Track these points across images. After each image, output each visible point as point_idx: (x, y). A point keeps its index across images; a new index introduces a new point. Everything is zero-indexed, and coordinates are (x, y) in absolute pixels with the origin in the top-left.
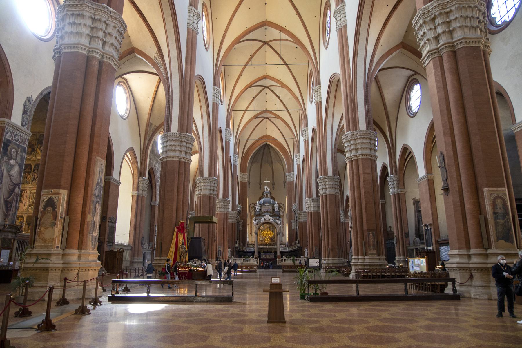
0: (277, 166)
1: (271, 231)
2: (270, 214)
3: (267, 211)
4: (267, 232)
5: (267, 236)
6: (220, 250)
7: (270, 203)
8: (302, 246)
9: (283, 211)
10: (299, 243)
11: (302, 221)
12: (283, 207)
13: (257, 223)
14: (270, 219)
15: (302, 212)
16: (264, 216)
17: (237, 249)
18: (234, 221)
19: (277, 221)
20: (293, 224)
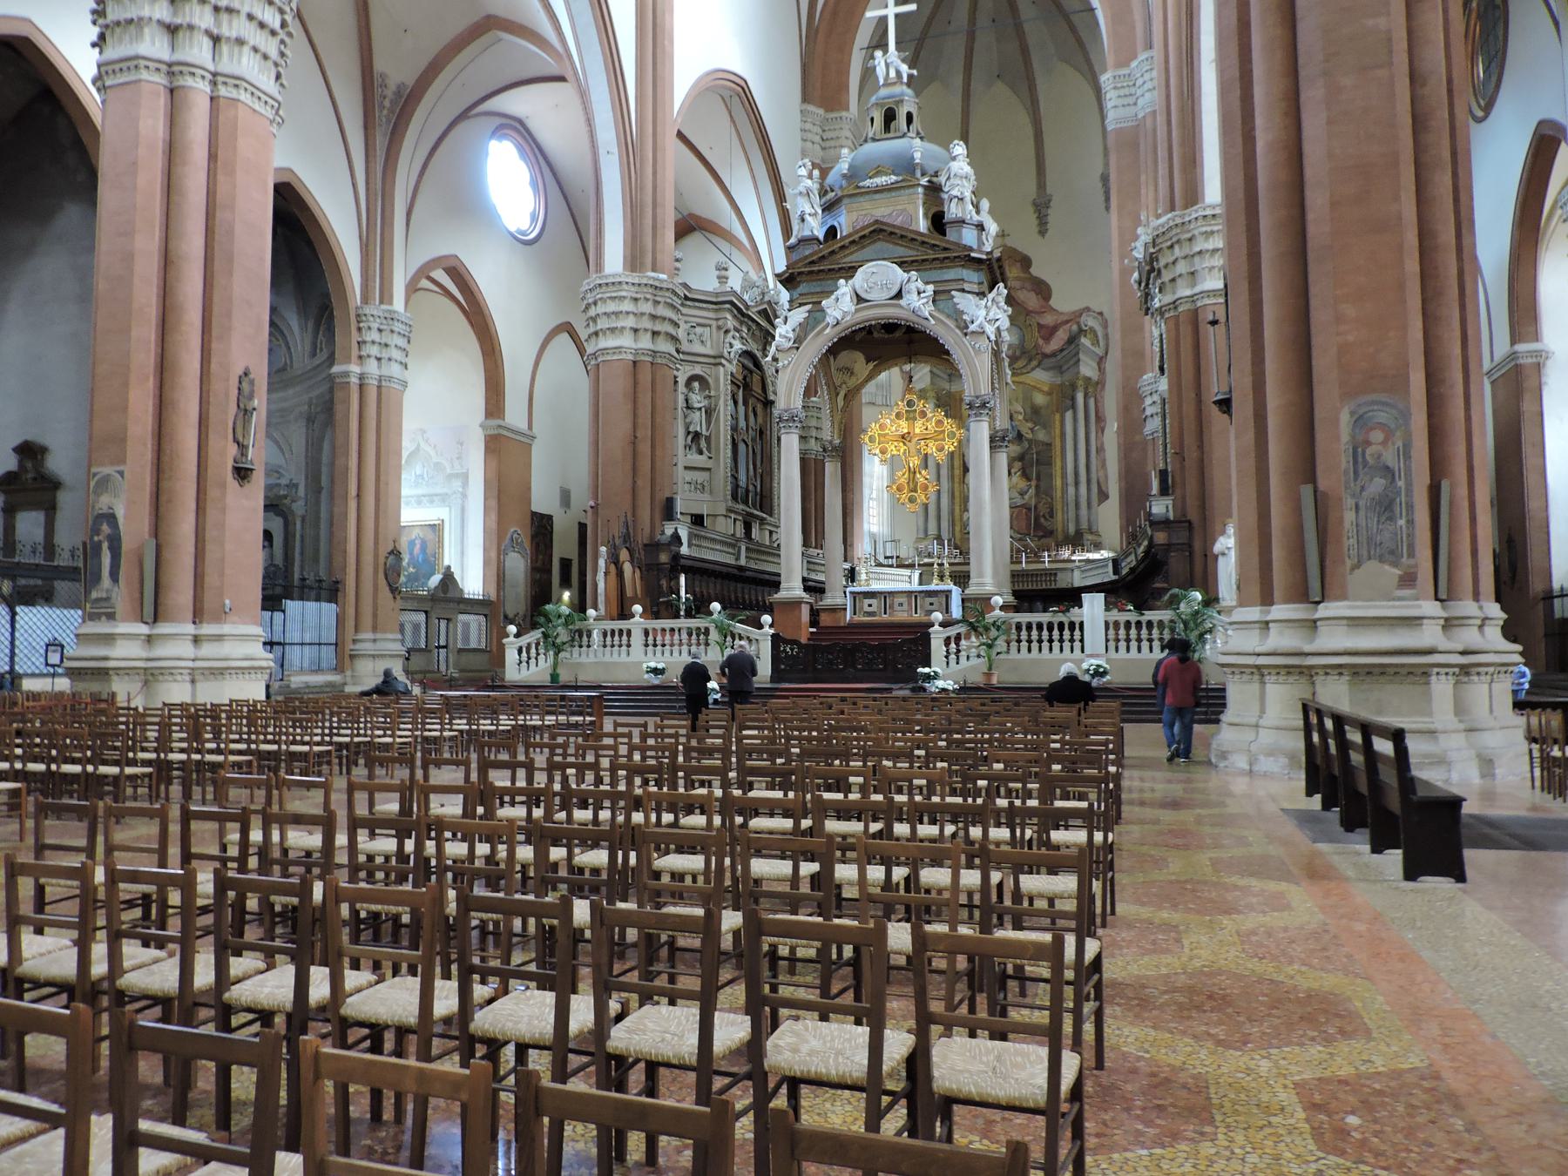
0: (1057, 83)
1: (940, 414)
2: (901, 251)
3: (878, 234)
4: (911, 418)
5: (907, 454)
6: (111, 518)
7: (907, 167)
8: (1193, 515)
9: (1100, 351)
10: (1164, 491)
11: (1192, 298)
12: (1100, 334)
13: (799, 341)
14: (899, 295)
15: (1194, 212)
16: (850, 272)
17: (664, 558)
18: (645, 342)
19: (966, 303)
20: (1151, 407)
